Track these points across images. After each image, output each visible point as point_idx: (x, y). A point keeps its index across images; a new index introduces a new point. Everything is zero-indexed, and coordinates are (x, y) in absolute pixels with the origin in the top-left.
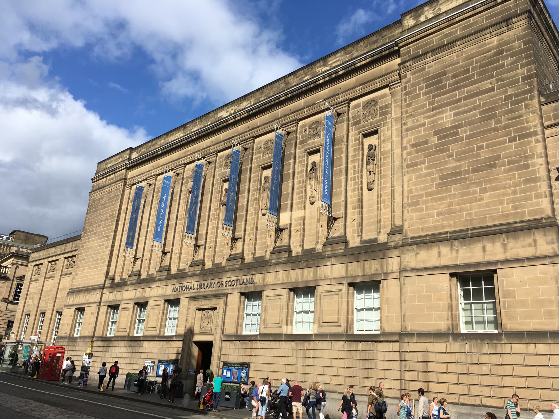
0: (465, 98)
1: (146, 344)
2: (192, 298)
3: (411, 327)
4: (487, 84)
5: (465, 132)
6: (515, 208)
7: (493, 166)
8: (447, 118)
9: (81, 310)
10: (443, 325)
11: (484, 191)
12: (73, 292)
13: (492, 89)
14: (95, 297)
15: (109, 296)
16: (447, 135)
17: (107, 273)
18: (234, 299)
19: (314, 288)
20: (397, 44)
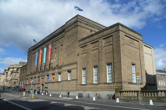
0: (71, 40)
1: (36, 85)
2: (41, 76)
3: (64, 80)
4: (73, 38)
5: (70, 46)
6: (74, 60)
7: (72, 53)
8: (69, 44)
9: (27, 79)
10: (66, 79)
11: (71, 57)
12: (27, 76)
13: (73, 39)
14: (29, 77)
15: (31, 76)
16: (68, 47)
17: (31, 72)
18: (46, 76)
19: (71, 71)
20: (64, 29)
